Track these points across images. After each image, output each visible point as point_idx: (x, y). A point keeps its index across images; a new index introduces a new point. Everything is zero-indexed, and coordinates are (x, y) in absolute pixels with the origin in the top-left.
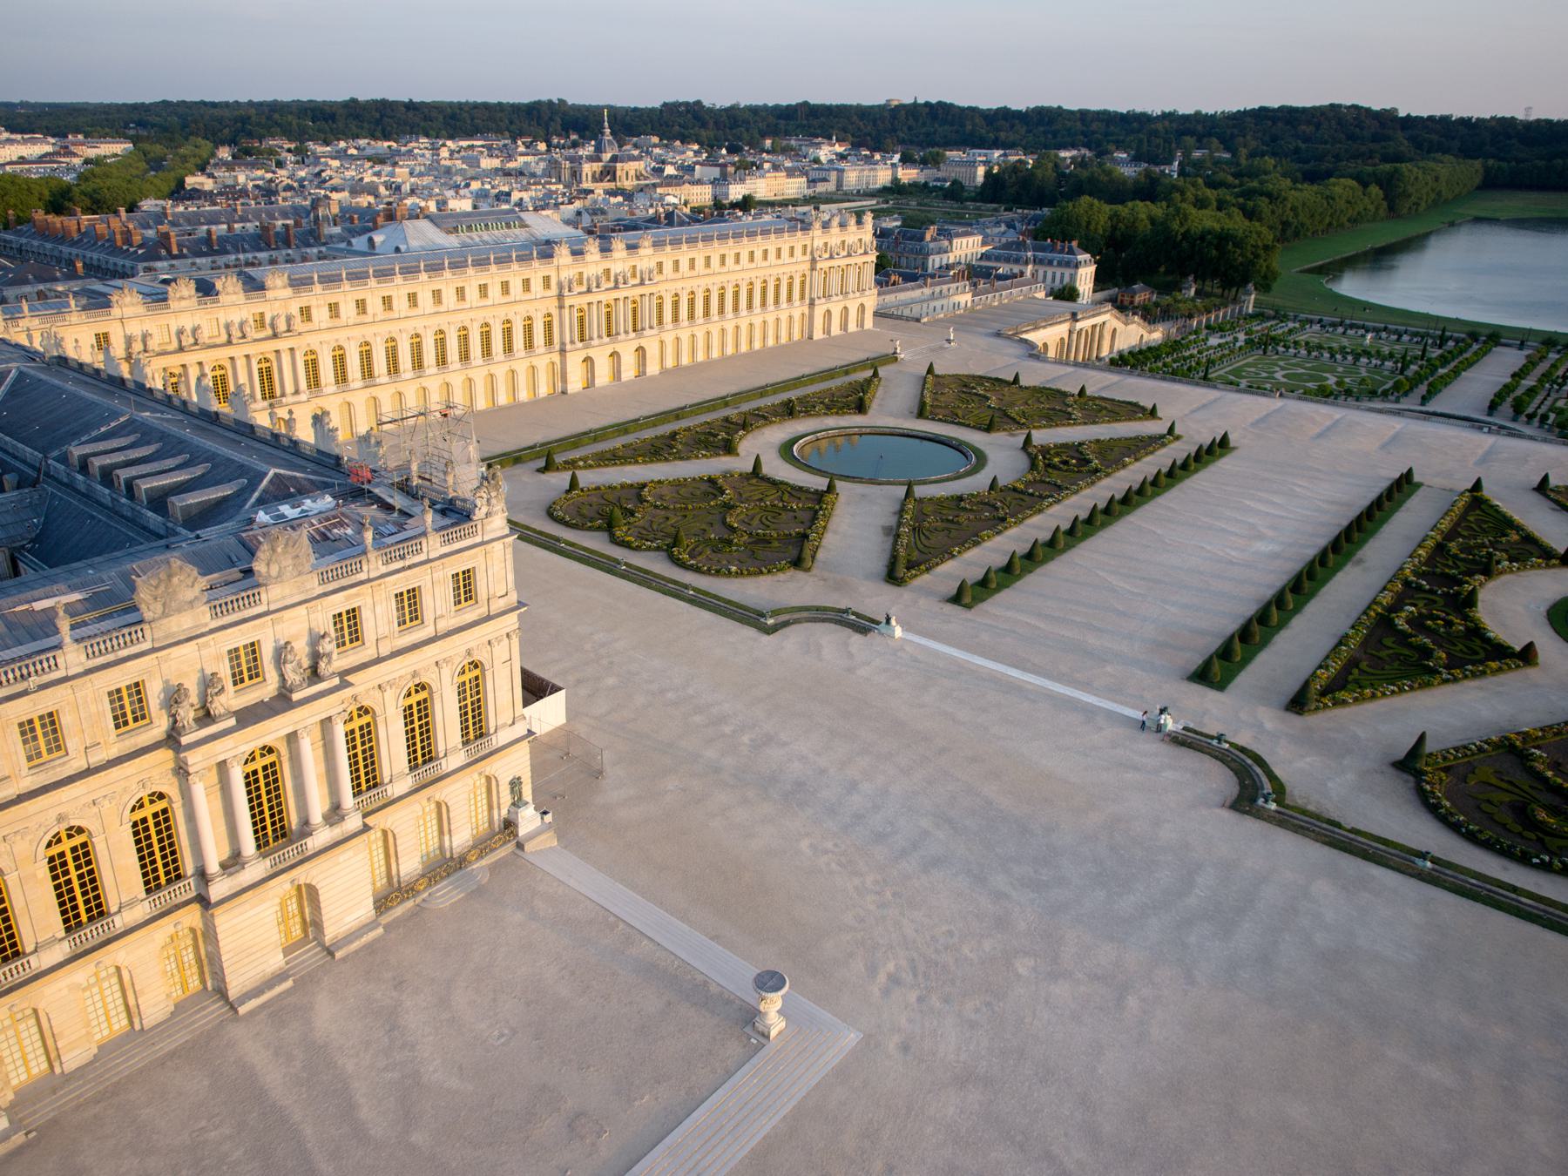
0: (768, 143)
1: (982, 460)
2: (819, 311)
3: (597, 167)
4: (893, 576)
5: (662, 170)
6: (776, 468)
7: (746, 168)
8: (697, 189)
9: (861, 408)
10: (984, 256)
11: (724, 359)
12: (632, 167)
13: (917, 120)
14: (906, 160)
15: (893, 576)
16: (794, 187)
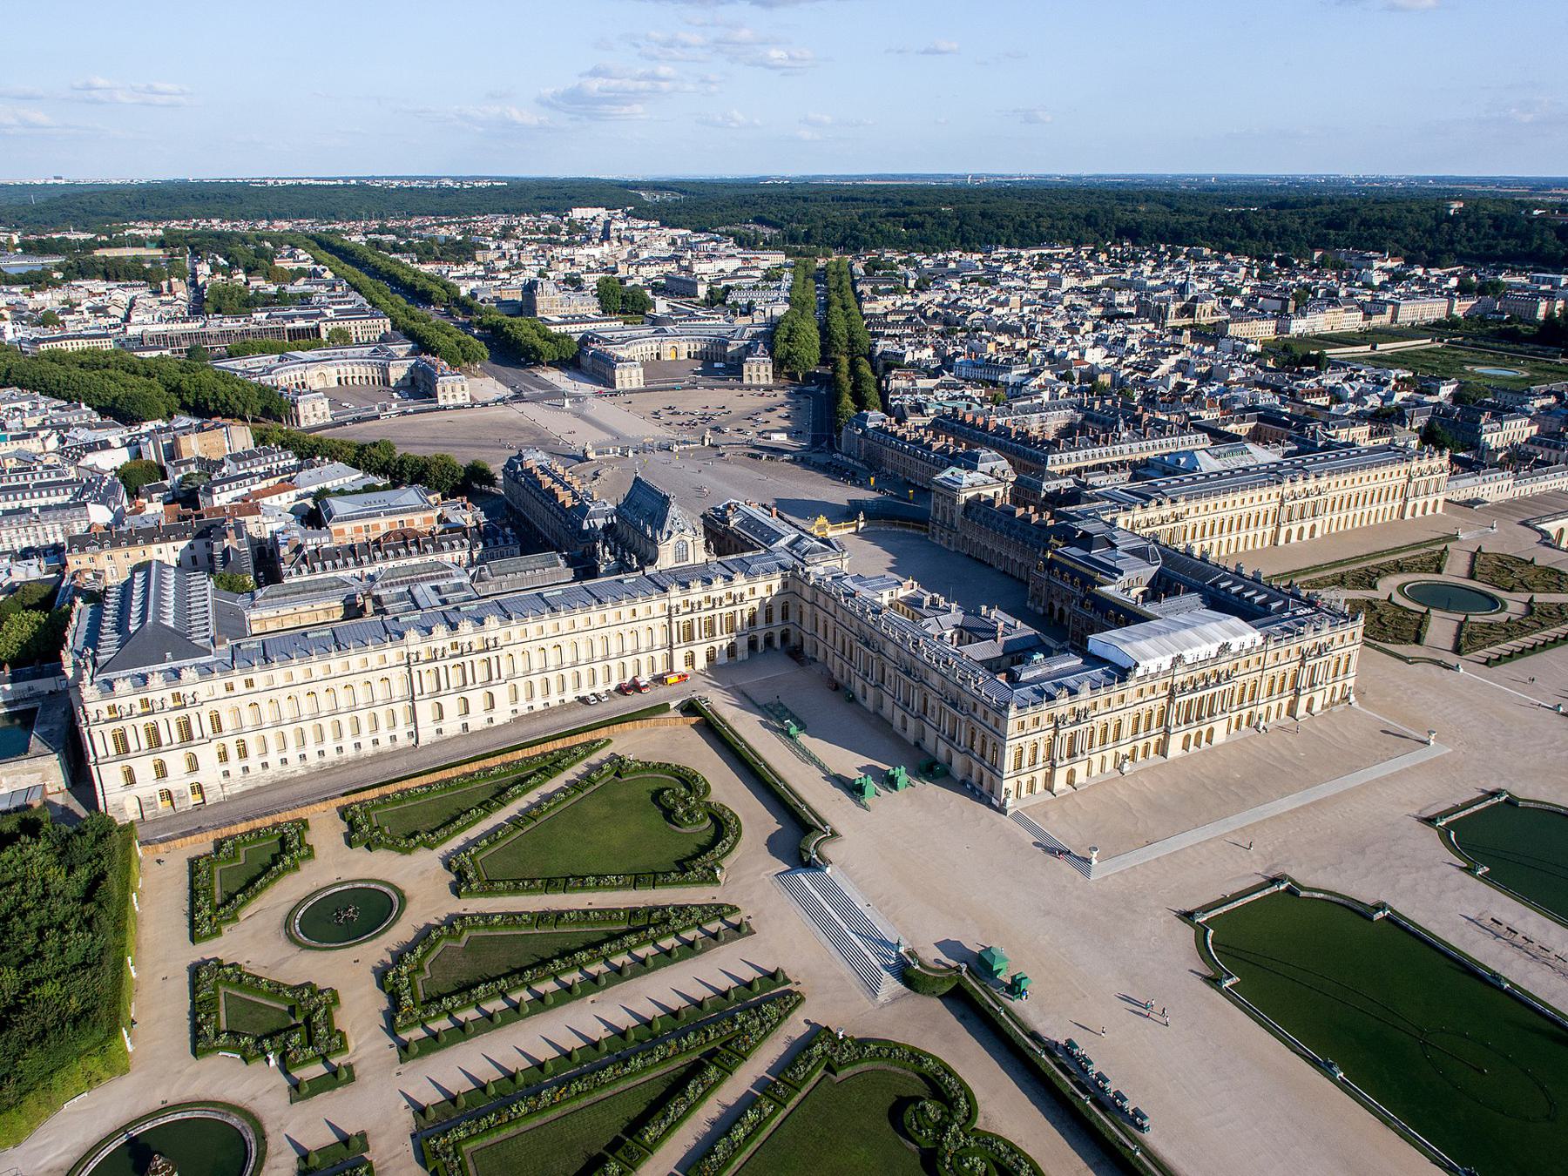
0: (1317, 254)
1: (1504, 606)
2: (1410, 505)
3: (1179, 305)
4: (1457, 650)
5: (1229, 302)
6: (1399, 600)
7: (1304, 301)
8: (1263, 324)
9: (1439, 571)
10: (1531, 441)
11: (1354, 530)
12: (1209, 305)
13: (1478, 232)
14: (1464, 290)
15: (1457, 650)
16: (1351, 321)
